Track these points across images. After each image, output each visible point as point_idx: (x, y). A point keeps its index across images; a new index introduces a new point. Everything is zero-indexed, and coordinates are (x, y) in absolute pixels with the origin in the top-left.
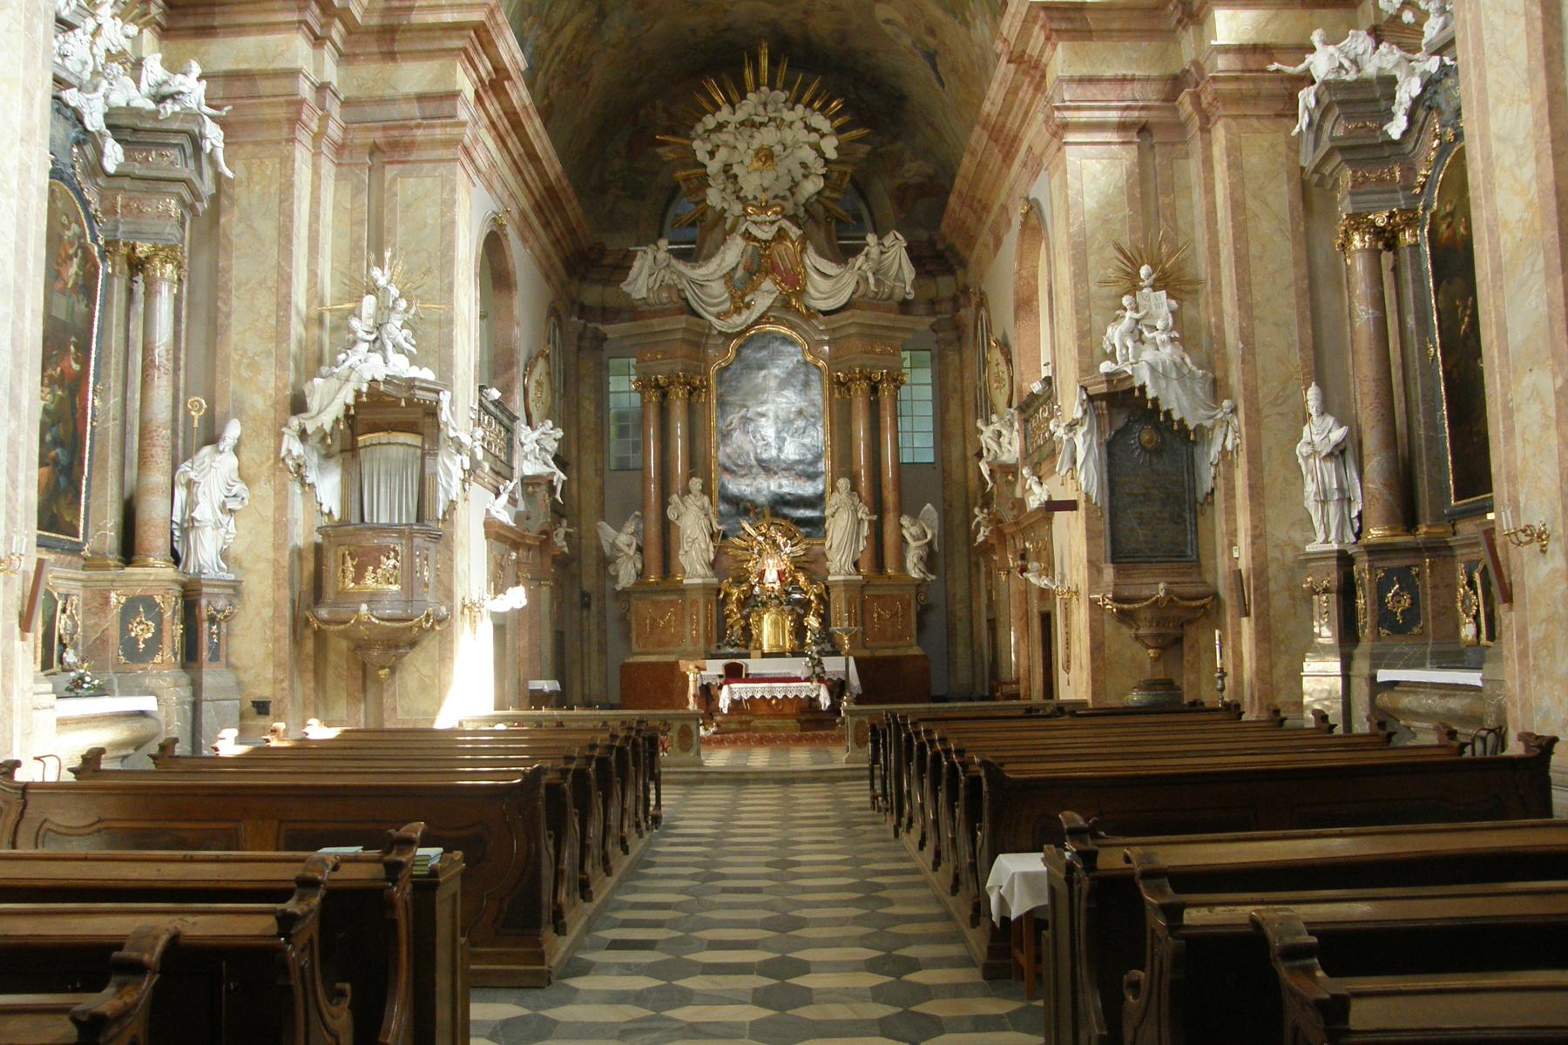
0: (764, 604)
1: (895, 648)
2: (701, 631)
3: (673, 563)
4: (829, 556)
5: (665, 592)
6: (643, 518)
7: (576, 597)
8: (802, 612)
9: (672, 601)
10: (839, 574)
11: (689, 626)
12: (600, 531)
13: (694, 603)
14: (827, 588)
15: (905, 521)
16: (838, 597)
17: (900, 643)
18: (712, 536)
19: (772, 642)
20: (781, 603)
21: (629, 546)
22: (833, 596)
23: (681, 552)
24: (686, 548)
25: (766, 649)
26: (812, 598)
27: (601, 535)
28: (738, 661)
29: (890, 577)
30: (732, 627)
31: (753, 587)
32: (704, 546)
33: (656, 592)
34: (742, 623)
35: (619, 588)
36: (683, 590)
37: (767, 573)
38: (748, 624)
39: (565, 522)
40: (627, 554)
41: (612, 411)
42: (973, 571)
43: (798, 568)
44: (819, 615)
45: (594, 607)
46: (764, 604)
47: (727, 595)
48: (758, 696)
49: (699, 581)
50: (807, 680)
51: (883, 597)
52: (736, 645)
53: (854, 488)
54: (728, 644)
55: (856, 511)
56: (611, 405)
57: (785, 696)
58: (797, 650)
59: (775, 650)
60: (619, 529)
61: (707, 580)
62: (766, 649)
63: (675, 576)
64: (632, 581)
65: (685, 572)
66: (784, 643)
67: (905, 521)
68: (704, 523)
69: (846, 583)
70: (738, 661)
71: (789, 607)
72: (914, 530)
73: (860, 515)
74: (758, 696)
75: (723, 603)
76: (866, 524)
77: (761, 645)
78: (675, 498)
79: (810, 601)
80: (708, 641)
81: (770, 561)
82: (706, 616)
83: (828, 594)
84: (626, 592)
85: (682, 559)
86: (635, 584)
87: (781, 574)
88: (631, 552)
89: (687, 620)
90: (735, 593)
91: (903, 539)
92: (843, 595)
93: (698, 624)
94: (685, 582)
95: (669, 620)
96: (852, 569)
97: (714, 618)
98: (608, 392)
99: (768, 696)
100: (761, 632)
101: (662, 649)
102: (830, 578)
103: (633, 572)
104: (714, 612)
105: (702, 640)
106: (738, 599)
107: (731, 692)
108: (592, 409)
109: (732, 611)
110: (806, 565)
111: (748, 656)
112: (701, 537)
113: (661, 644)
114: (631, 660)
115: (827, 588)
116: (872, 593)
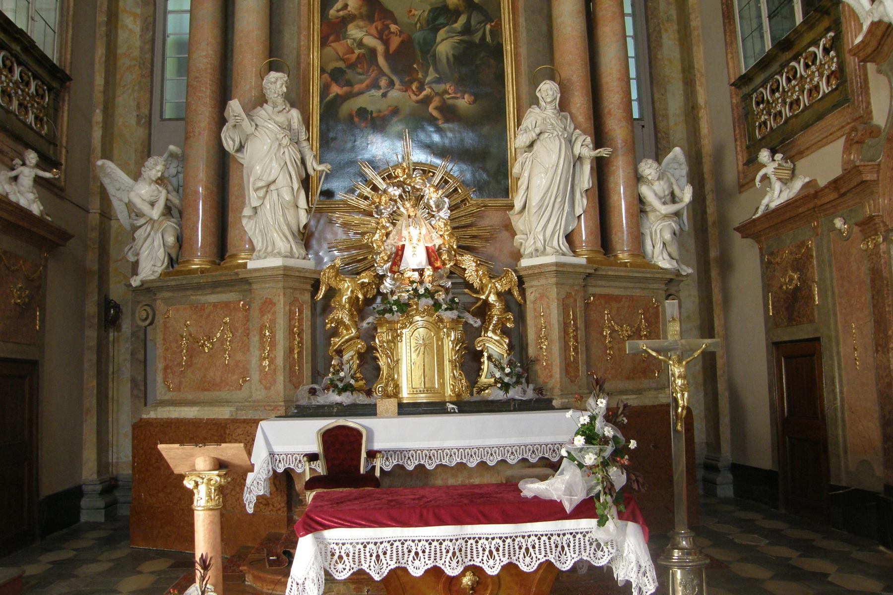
0: (404, 307)
1: (639, 392)
2: (280, 361)
3: (232, 234)
4: (519, 223)
5: (215, 286)
6: (182, 159)
7: (92, 308)
8: (476, 322)
9: (226, 304)
10: (544, 253)
11: (255, 353)
12: (106, 181)
13: (268, 304)
14: (521, 281)
15: (648, 168)
16: (542, 296)
17: (645, 383)
18: (306, 182)
19: (418, 383)
20: (437, 306)
21: (152, 204)
22: (531, 296)
23: (247, 212)
24: (255, 203)
25: (406, 395)
26: (492, 298)
27: (111, 190)
28: (352, 422)
29: (625, 264)
30: (340, 352)
31: (381, 278)
32: (287, 197)
33: (199, 288)
34: (361, 345)
35: (135, 282)
36: (246, 281)
37: (407, 253)
38: (371, 349)
39: (32, 157)
40: (151, 220)
41: (170, 40)
42: (714, 273)
43: (465, 249)
44: (505, 332)
45: (126, 326)
46: (404, 307)
47: (332, 293)
48: (417, 569)
49: (277, 262)
50: (585, 509)
51: (618, 299)
52: (348, 388)
53: (563, 106)
54: (333, 386)
55: (570, 142)
56: (170, 29)
57: (511, 568)
58: (466, 397)
59: (422, 398)
60: (136, 176)
61: (291, 262)
62: (406, 395)
63: (234, 256)
64: (159, 270)
65: (253, 249)
66: (442, 385)
67: (648, 168)
68: (290, 154)
69: (560, 270)
70: (352, 422)
71: (453, 314)
72: (660, 187)
73: (577, 150)
74: (417, 569)
75: (326, 307)
76: (587, 168)
77: (397, 386)
78: (234, 106)
79: (486, 304)
80: (294, 380)
81: (414, 231)
82: (291, 332)
83: (523, 292)
84: (148, 289)
85: (248, 225)
86: (165, 274)
87: (432, 255)
88: (156, 213)
89: (255, 339)
90: (347, 288)
91: (640, 207)
92: (553, 293)
93: (273, 344)
94: (251, 265)
95: (222, 341)
96: (565, 247)
97: (307, 337)
98: (165, 13)
99: (452, 571)
100: (395, 364)
101: (208, 395)
102: (524, 263)
103: (161, 253)
104: (307, 325)
105: (280, 378)
106: (354, 301)
107: (328, 554)
108: (137, 29)
109: (340, 322)
110: (476, 243)
111: (370, 411)
112: (283, 180)
113: (206, 385)
114: (152, 415)
115: (521, 281)
116: (597, 290)
